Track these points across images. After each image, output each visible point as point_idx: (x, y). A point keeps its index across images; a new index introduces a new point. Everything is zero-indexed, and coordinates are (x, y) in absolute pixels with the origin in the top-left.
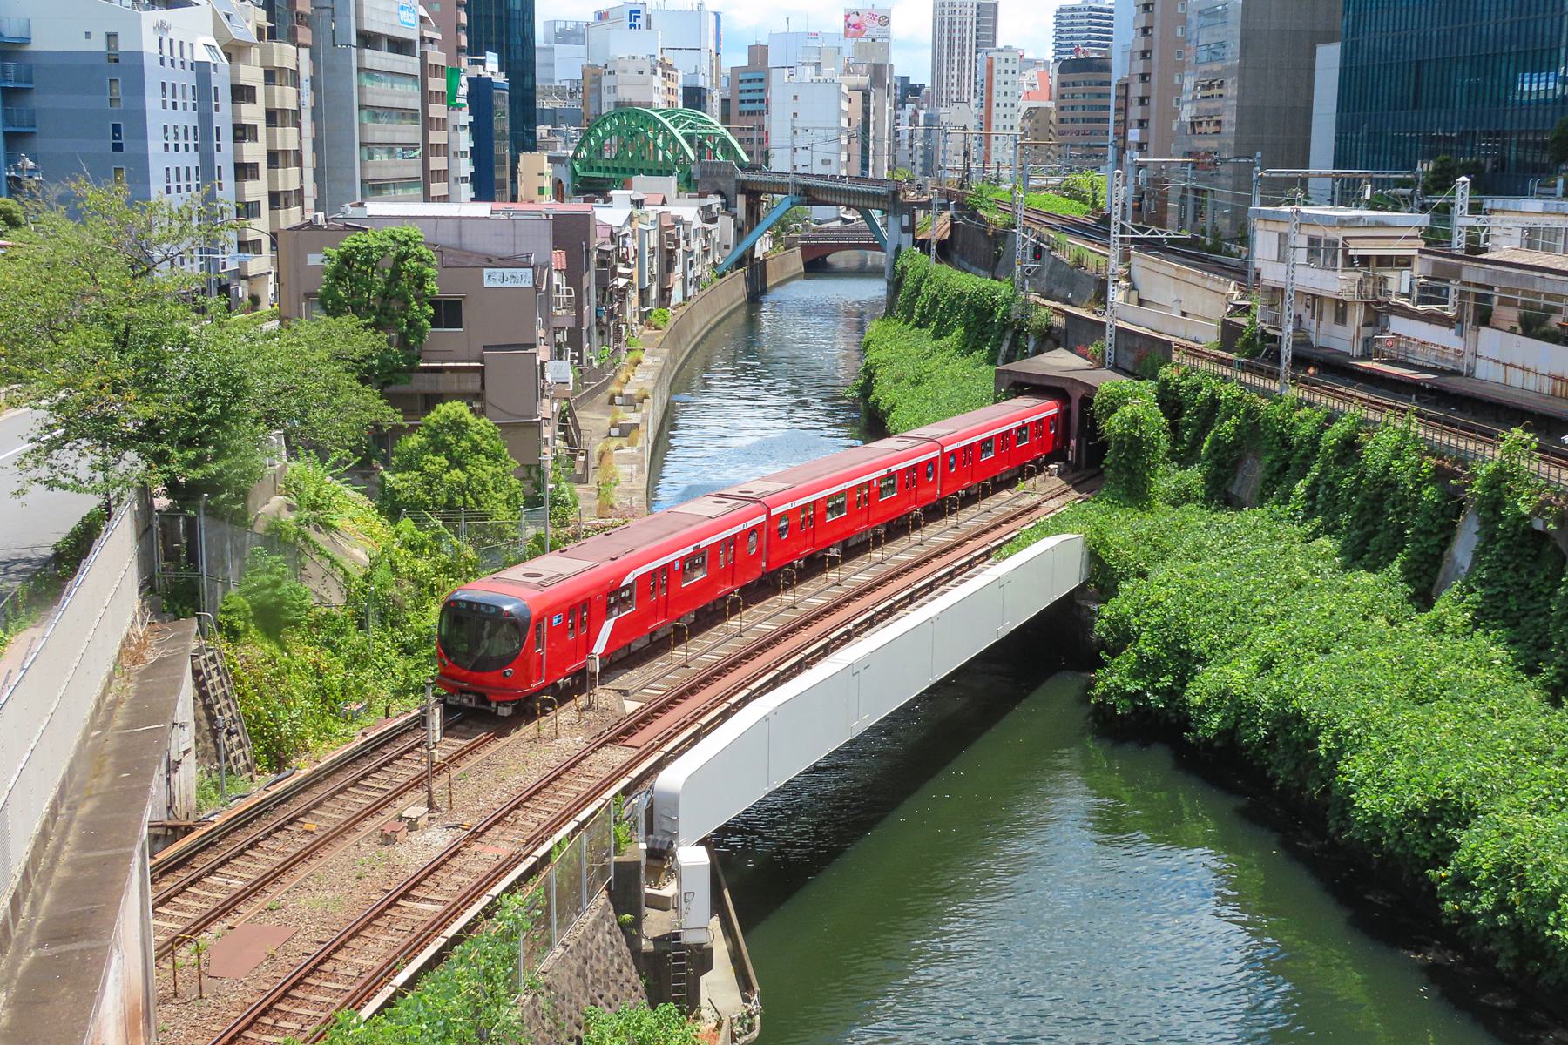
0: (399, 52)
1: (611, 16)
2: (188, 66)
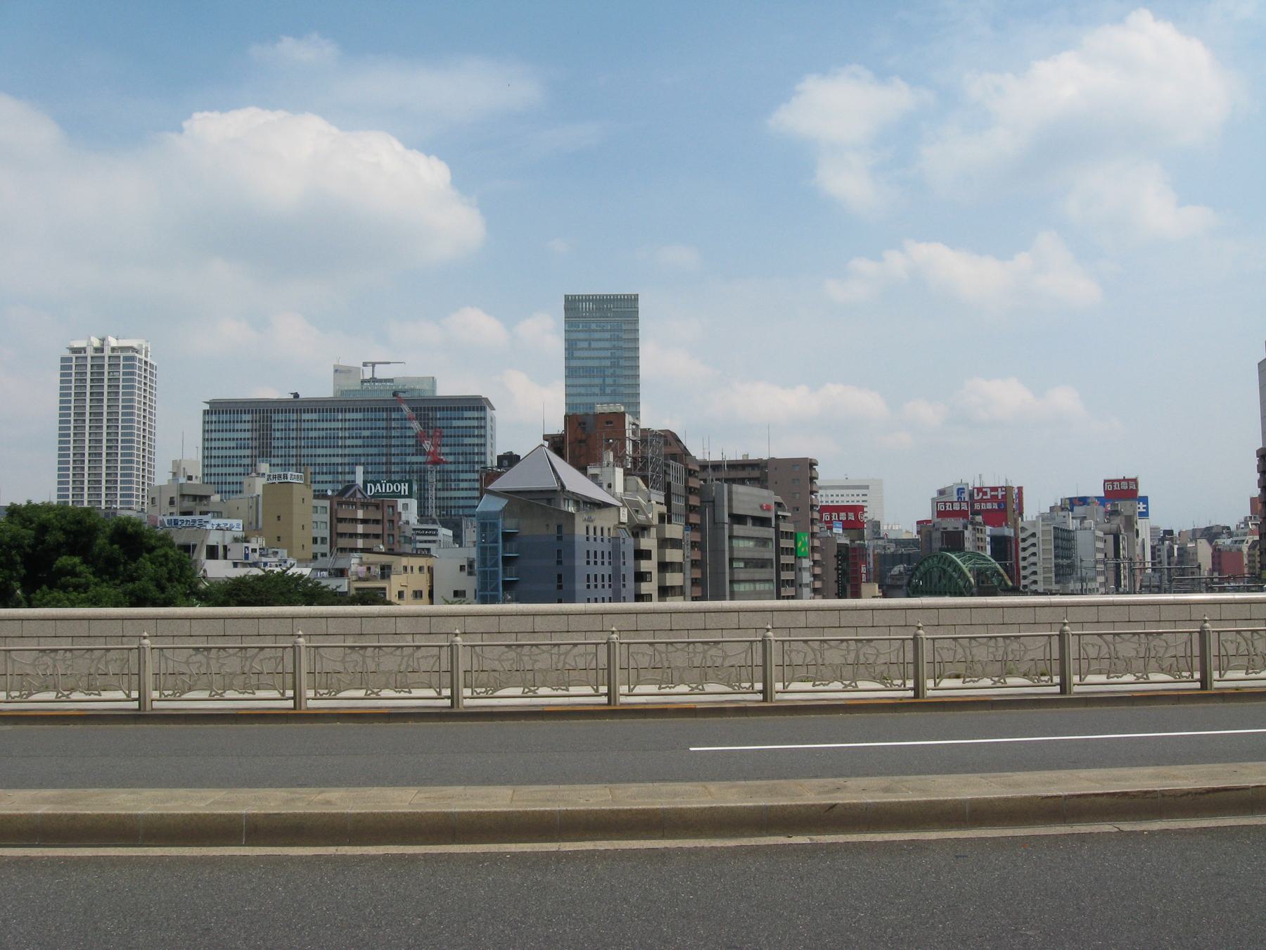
0: (762, 525)
1: (947, 492)
2: (606, 540)
